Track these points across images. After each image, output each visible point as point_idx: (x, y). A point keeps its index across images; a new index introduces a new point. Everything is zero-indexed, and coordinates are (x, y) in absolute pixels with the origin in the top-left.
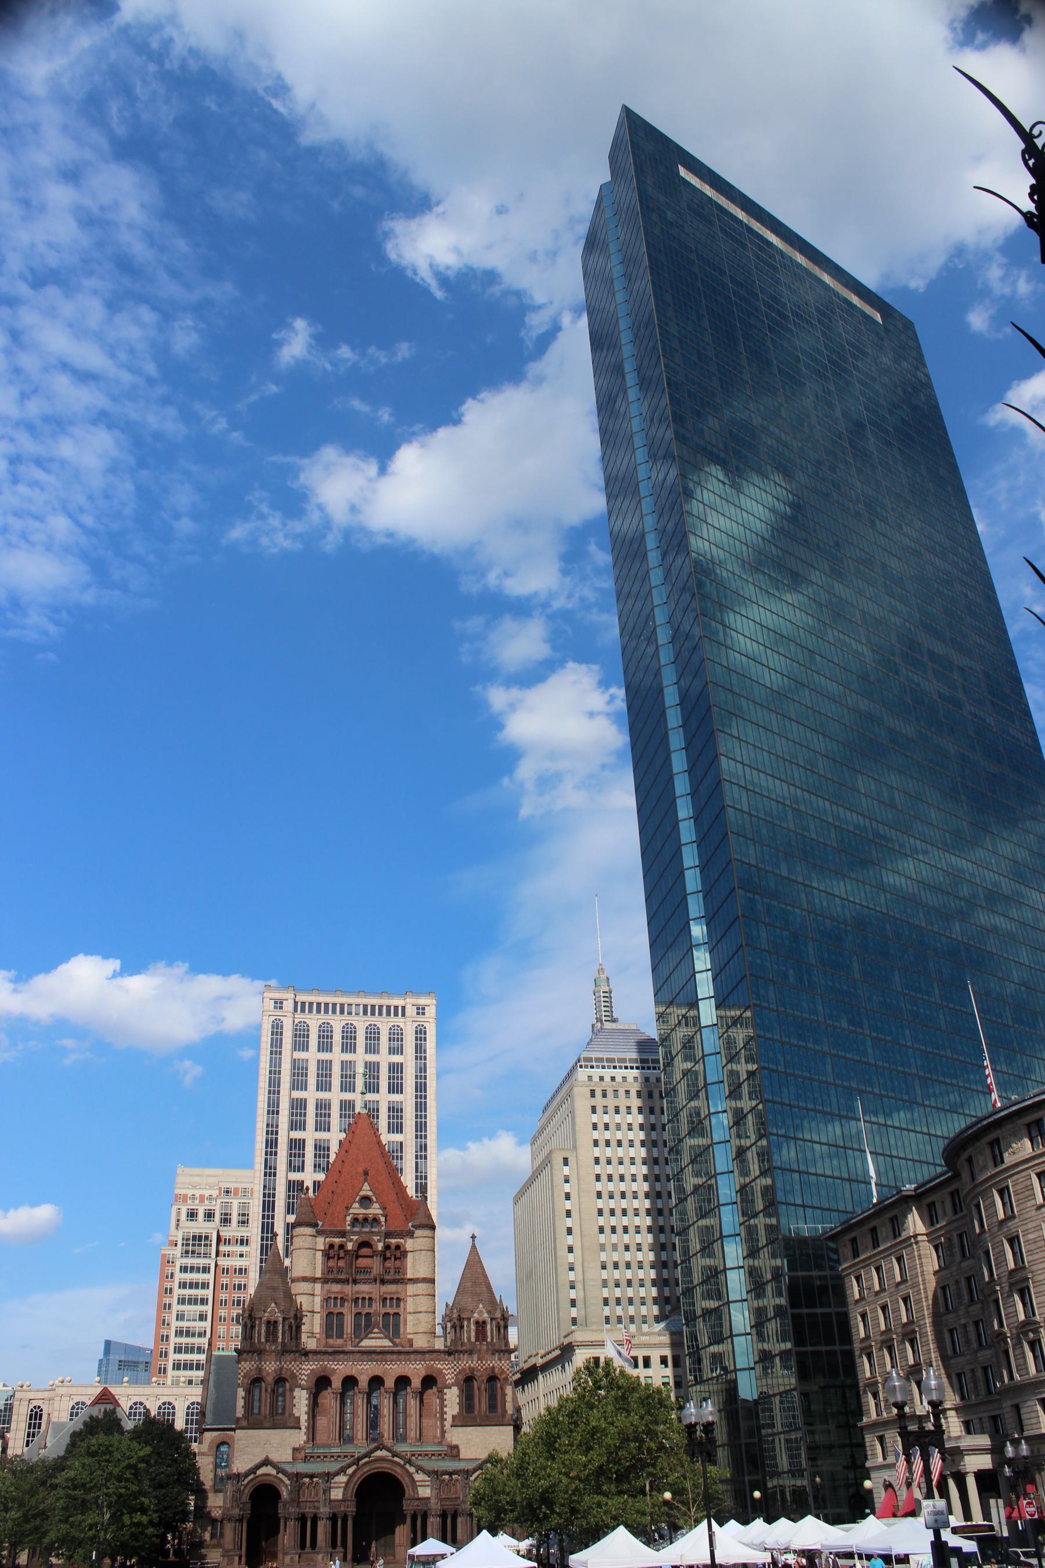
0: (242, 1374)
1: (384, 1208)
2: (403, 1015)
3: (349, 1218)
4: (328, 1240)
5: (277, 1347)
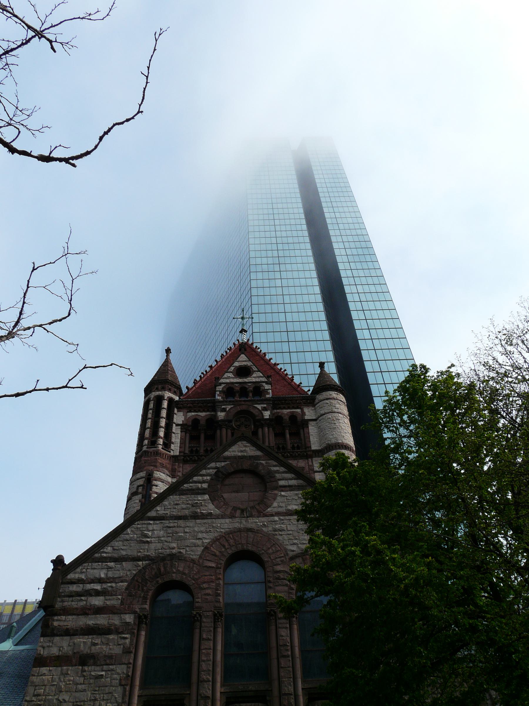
1: (268, 377)
3: (220, 388)
4: (190, 414)
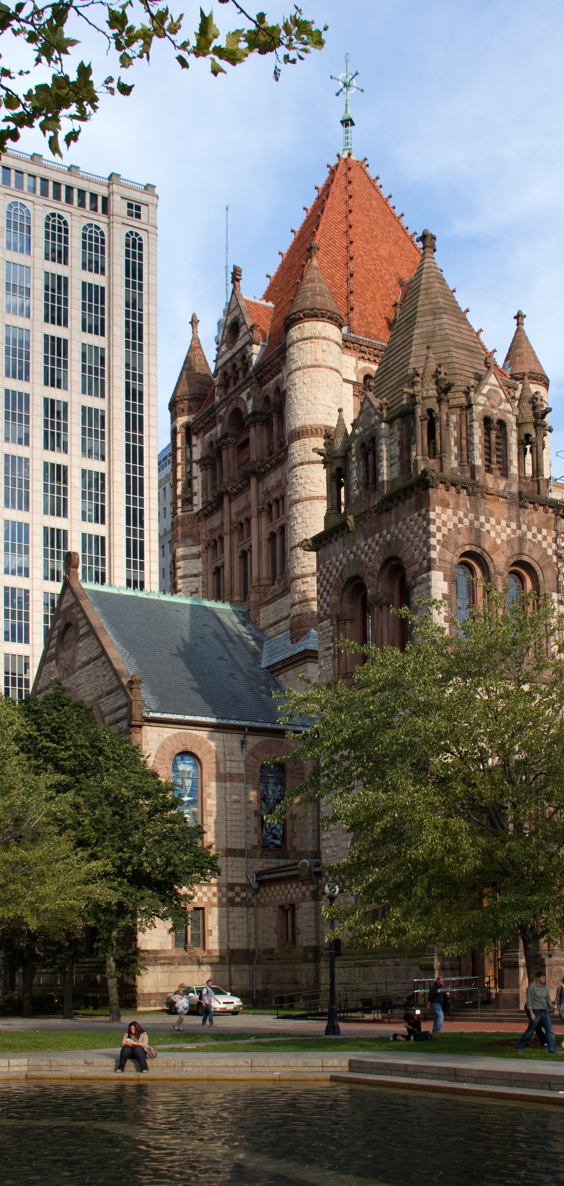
0: (439, 536)
2: (105, 211)
5: (508, 486)
